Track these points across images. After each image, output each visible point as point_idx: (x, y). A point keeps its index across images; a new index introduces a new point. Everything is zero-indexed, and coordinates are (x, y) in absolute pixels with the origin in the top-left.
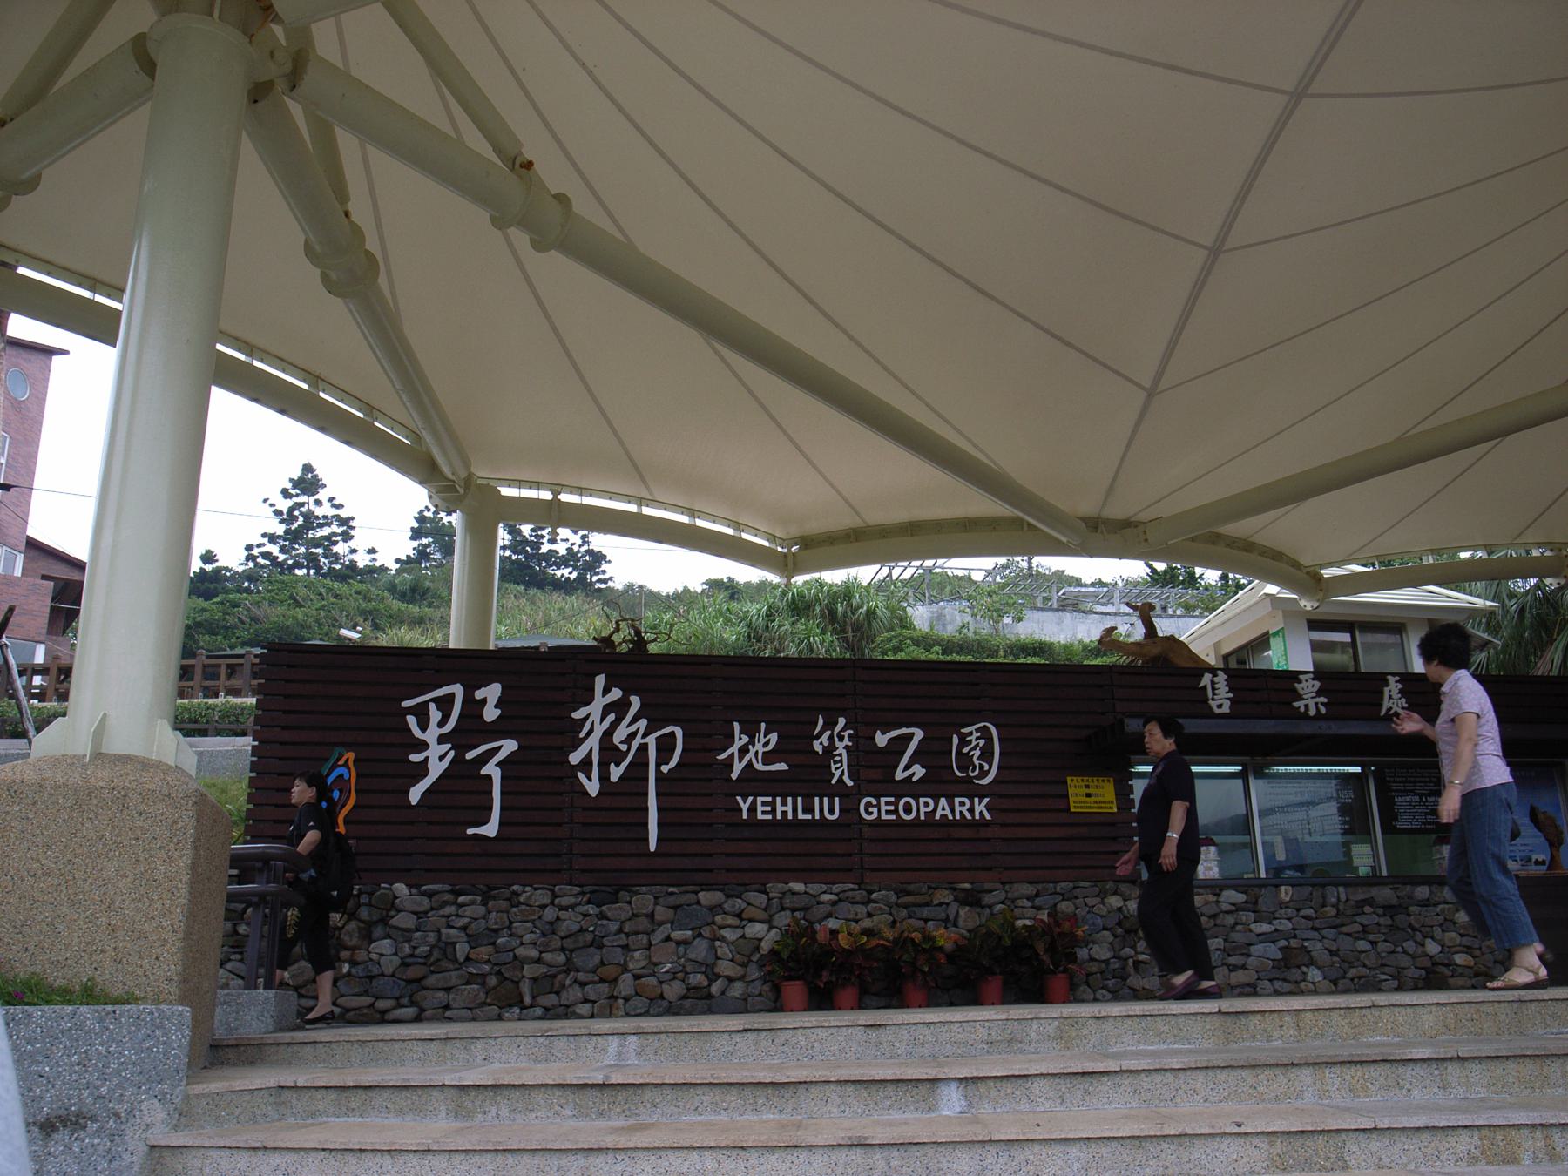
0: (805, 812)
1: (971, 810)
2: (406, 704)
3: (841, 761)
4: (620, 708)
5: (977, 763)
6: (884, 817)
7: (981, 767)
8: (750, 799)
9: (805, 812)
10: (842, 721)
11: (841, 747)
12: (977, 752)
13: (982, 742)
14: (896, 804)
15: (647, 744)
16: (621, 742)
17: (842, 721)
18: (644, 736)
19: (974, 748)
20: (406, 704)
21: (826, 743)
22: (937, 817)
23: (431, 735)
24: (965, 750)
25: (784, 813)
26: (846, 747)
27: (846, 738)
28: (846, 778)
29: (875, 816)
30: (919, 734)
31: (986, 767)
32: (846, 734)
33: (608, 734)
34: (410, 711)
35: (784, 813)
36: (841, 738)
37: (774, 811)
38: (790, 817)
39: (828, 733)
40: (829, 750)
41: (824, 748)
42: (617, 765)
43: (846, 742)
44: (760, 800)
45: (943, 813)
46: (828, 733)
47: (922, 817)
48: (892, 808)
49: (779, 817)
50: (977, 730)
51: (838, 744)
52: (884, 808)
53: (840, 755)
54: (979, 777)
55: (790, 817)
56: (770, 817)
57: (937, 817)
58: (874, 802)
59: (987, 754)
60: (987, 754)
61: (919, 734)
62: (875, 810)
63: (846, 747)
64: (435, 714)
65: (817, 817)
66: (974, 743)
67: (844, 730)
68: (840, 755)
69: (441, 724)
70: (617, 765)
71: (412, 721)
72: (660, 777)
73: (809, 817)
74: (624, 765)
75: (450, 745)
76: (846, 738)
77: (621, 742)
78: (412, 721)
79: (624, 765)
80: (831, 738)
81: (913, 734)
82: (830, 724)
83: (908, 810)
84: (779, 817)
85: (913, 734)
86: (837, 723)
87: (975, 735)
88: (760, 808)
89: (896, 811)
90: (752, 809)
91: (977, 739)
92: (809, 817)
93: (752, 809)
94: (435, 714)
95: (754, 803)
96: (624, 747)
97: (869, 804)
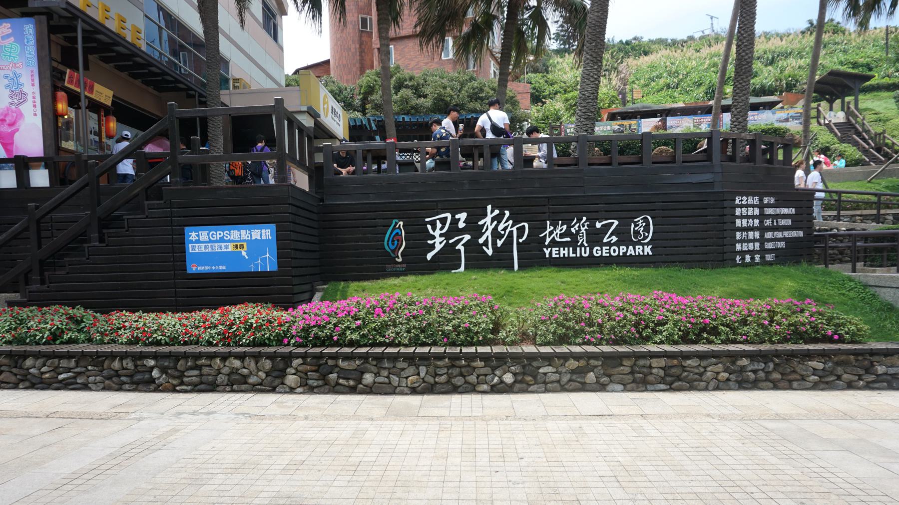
0: (573, 253)
1: (643, 251)
2: (427, 220)
3: (583, 236)
4: (498, 219)
5: (642, 233)
6: (604, 254)
7: (644, 234)
8: (549, 249)
9: (573, 253)
10: (584, 219)
11: (583, 230)
12: (642, 229)
13: (644, 224)
14: (609, 249)
15: (512, 231)
16: (502, 230)
17: (584, 219)
18: (511, 228)
19: (640, 227)
20: (427, 220)
21: (577, 229)
22: (628, 254)
23: (437, 233)
24: (636, 229)
25: (564, 254)
26: (586, 230)
27: (586, 226)
28: (585, 243)
29: (599, 254)
30: (616, 223)
31: (647, 234)
32: (586, 224)
33: (496, 228)
34: (429, 223)
35: (564, 254)
36: (583, 226)
37: (559, 254)
38: (566, 256)
39: (578, 224)
40: (578, 232)
41: (576, 231)
42: (500, 240)
43: (586, 227)
44: (554, 249)
45: (631, 253)
46: (578, 224)
47: (621, 254)
48: (608, 251)
49: (562, 256)
50: (641, 219)
51: (582, 228)
52: (604, 251)
53: (583, 233)
54: (644, 239)
55: (566, 256)
56: (558, 256)
57: (628, 254)
58: (599, 248)
59: (647, 229)
60: (647, 229)
61: (616, 223)
62: (599, 252)
63: (586, 230)
64: (439, 225)
65: (578, 255)
66: (640, 225)
67: (585, 222)
68: (583, 233)
69: (441, 229)
70: (500, 240)
71: (429, 227)
72: (518, 243)
73: (574, 255)
74: (503, 240)
75: (444, 238)
76: (586, 226)
77: (502, 230)
78: (429, 227)
79: (503, 240)
80: (579, 227)
81: (614, 223)
82: (579, 220)
83: (614, 251)
84: (562, 256)
85: (614, 223)
86: (582, 219)
87: (641, 221)
88: (554, 252)
89: (609, 253)
90: (551, 253)
91: (642, 223)
92: (574, 255)
93: (551, 253)
94: (439, 225)
95: (551, 250)
96: (503, 232)
97: (597, 250)
